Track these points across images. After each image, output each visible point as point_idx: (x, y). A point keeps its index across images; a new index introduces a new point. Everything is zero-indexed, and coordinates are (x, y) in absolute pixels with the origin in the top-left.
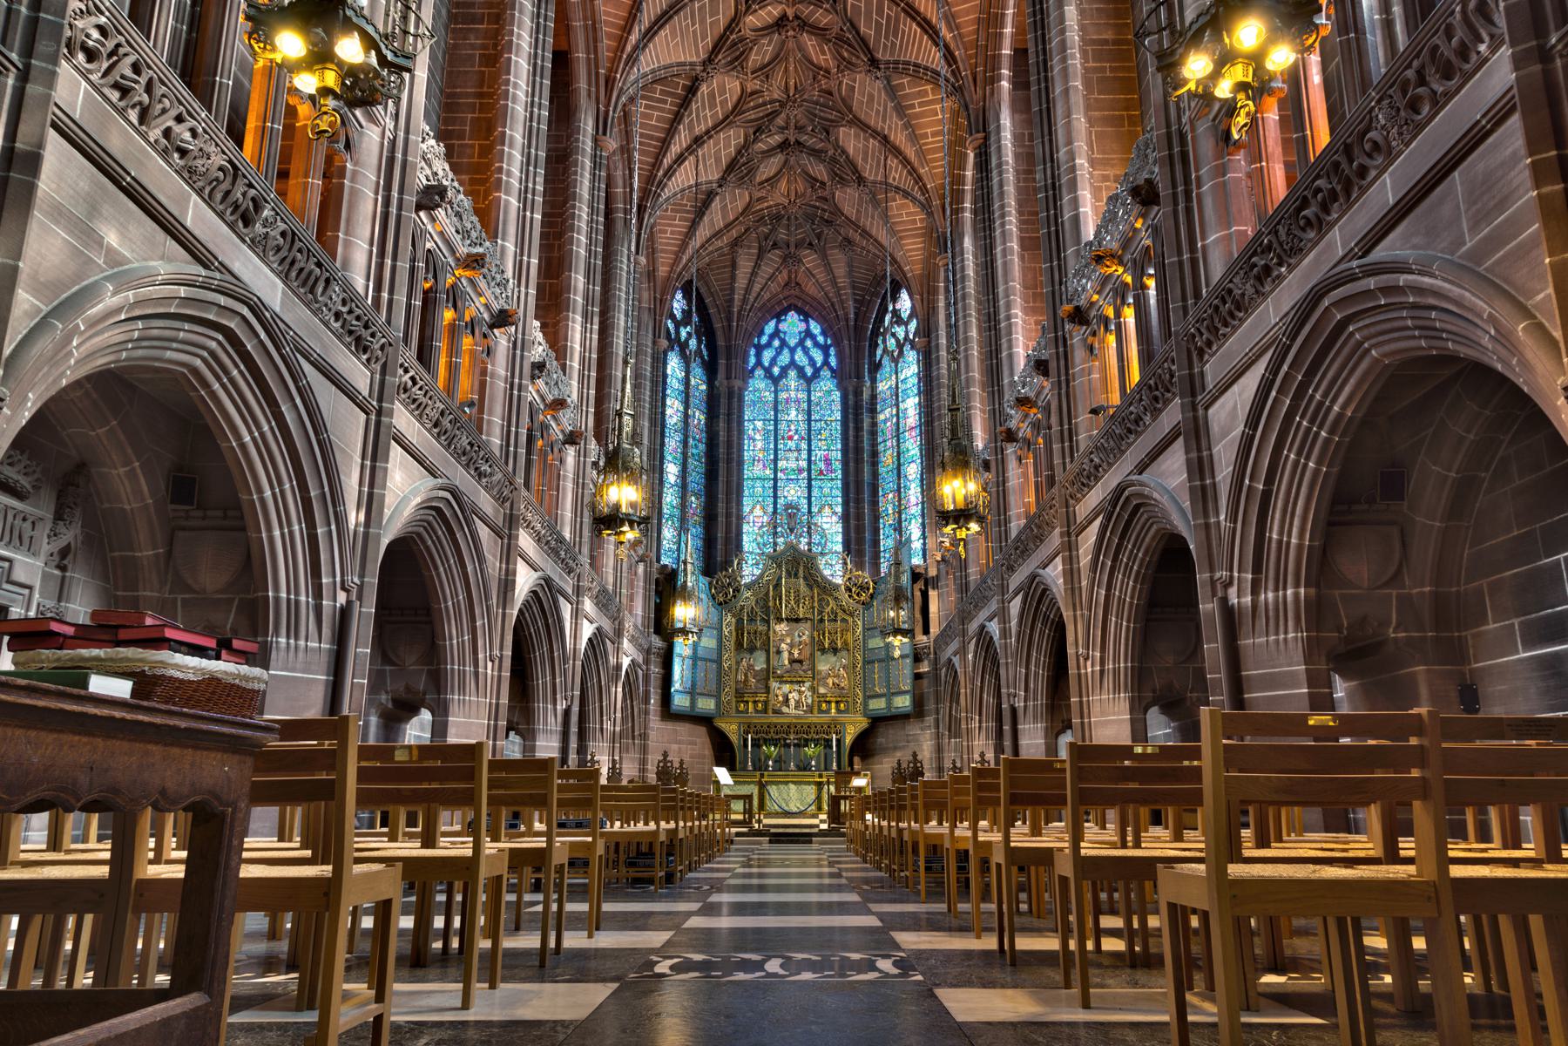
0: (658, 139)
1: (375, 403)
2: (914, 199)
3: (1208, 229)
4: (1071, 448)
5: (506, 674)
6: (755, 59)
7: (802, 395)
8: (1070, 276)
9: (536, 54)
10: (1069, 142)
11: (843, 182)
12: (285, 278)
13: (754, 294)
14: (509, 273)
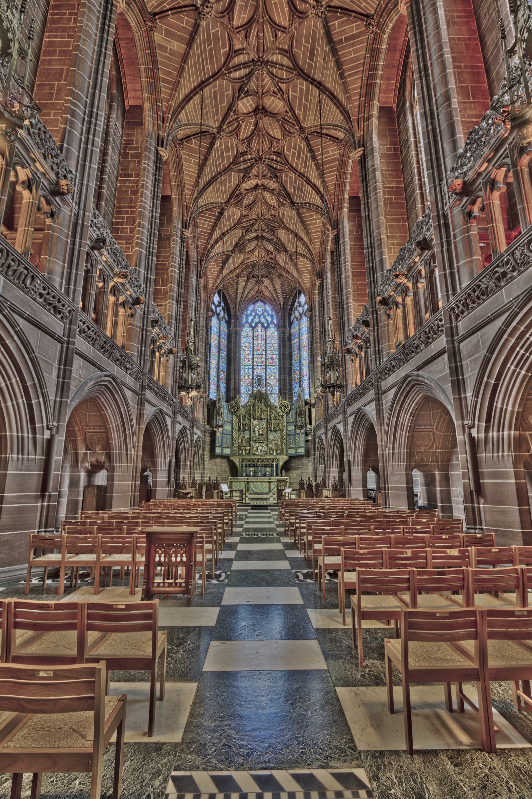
0: (208, 233)
1: (66, 339)
2: (307, 258)
3: (460, 259)
4: (379, 357)
5: (140, 453)
6: (246, 202)
7: (263, 334)
8: (379, 284)
9: (154, 191)
10: (378, 228)
11: (279, 252)
12: (6, 275)
13: (245, 295)
14: (141, 282)
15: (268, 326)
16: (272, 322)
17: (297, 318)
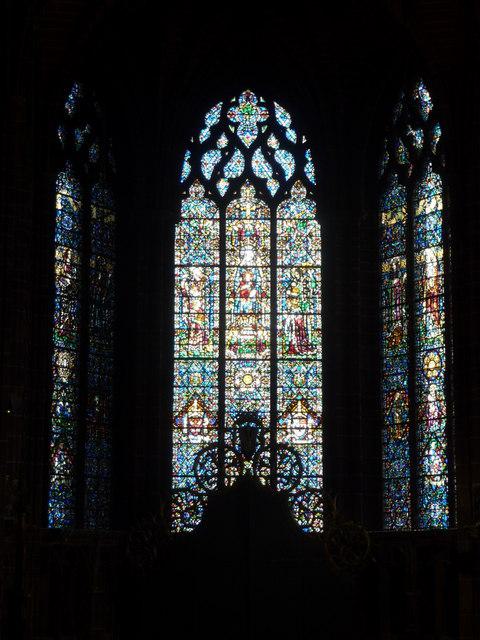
7: (263, 227)
15: (284, 194)
17: (402, 170)
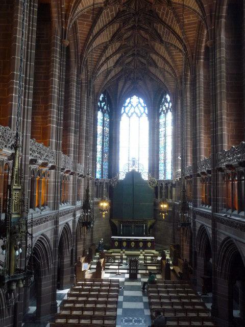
6: (125, 36)
15: (141, 116)
16: (144, 112)
17: (164, 111)
